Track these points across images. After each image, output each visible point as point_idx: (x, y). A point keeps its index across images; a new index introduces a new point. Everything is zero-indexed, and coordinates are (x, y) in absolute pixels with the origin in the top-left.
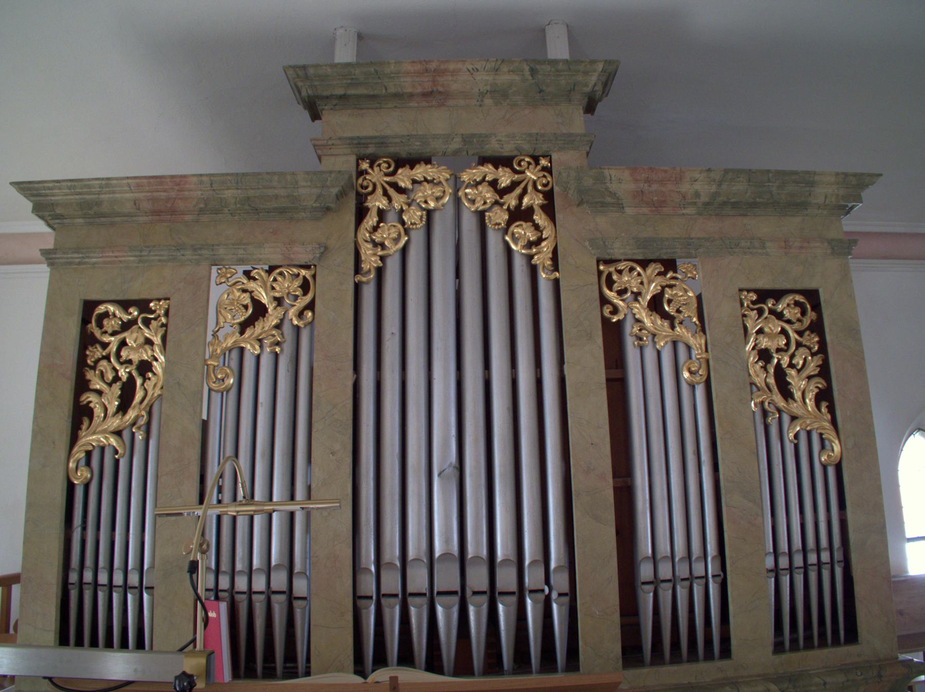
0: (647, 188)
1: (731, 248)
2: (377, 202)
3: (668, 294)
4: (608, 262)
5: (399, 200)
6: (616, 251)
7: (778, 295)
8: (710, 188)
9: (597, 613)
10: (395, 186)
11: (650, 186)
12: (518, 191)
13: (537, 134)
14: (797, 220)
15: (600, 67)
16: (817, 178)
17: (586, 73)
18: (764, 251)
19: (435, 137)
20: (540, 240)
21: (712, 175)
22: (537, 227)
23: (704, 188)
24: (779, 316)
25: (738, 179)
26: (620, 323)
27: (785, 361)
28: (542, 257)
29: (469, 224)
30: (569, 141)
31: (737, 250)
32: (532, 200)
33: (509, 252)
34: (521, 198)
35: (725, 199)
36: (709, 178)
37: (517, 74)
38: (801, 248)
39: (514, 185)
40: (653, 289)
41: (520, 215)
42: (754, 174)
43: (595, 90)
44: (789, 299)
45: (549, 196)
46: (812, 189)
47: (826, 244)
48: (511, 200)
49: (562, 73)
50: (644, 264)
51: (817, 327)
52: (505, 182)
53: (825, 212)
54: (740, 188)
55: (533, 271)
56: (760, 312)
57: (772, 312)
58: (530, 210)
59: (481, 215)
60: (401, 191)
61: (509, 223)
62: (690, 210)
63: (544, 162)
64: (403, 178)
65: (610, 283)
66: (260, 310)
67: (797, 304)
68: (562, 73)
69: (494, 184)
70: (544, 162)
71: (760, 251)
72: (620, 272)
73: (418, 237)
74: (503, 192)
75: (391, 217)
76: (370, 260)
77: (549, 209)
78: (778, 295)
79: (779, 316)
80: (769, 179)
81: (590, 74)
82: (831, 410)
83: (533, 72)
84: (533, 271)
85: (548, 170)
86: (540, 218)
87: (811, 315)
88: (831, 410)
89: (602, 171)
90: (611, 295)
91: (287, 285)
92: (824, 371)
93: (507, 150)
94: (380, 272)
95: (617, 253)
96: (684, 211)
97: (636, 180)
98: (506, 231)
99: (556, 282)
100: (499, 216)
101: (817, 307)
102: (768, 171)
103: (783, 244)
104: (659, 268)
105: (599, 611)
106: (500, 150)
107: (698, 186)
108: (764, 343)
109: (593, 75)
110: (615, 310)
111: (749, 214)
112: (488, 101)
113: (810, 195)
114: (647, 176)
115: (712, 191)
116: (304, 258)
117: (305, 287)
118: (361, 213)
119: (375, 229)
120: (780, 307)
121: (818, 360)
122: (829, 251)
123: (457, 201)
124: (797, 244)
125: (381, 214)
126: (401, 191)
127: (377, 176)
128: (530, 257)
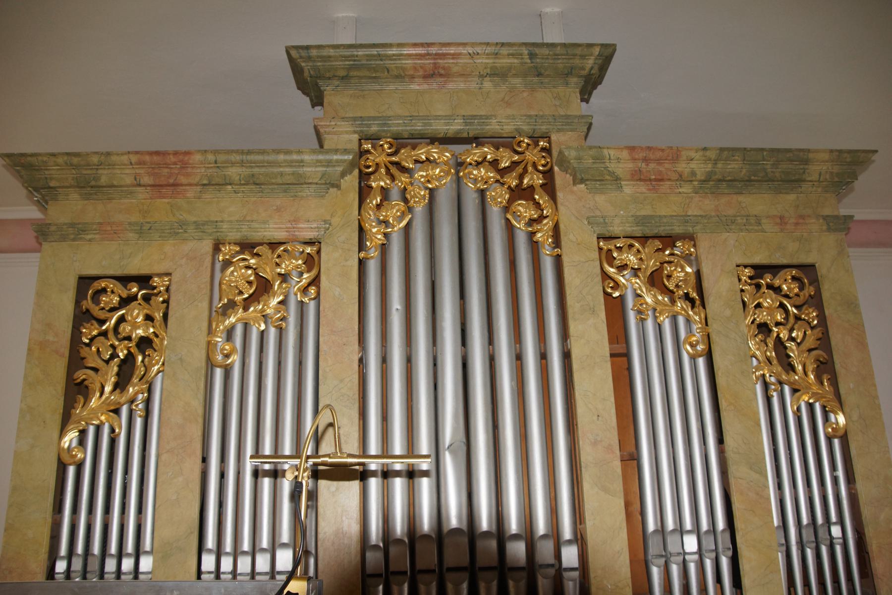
0: (645, 167)
1: (727, 225)
3: (668, 268)
6: (616, 228)
8: (705, 166)
9: (610, 587)
11: (647, 165)
12: (520, 169)
13: (536, 116)
14: (792, 197)
15: (597, 50)
16: (811, 156)
17: (583, 57)
18: (760, 228)
19: (437, 117)
20: (542, 217)
21: (708, 153)
22: (538, 205)
23: (700, 168)
24: (777, 290)
25: (733, 158)
27: (784, 335)
30: (567, 122)
31: (733, 227)
32: (534, 179)
33: (510, 229)
34: (521, 177)
35: (720, 177)
36: (706, 156)
37: (517, 58)
38: (797, 224)
39: (515, 164)
40: (652, 264)
41: (521, 193)
42: (748, 153)
43: (591, 73)
44: (789, 274)
45: (548, 174)
46: (806, 167)
47: (821, 221)
49: (560, 57)
50: (644, 239)
51: (816, 301)
52: (504, 164)
53: (819, 190)
54: (735, 166)
55: (534, 247)
56: (758, 286)
57: (770, 287)
58: (531, 188)
59: (482, 193)
60: (404, 170)
61: (510, 201)
62: (686, 189)
64: (406, 157)
65: (611, 260)
67: (794, 278)
68: (560, 57)
69: (494, 163)
71: (756, 228)
72: (619, 249)
74: (503, 172)
76: (376, 233)
77: (549, 188)
78: (774, 269)
79: (777, 290)
80: (763, 157)
81: (587, 57)
82: (834, 383)
83: (532, 56)
84: (534, 247)
87: (810, 290)
89: (602, 150)
92: (824, 342)
94: (384, 249)
95: (617, 230)
96: (681, 190)
97: (634, 159)
99: (558, 261)
100: (498, 196)
101: (815, 281)
102: (762, 150)
103: (778, 221)
105: (611, 585)
106: (501, 131)
107: (693, 165)
109: (590, 59)
110: (617, 286)
111: (744, 192)
113: (804, 172)
114: (645, 155)
115: (707, 170)
116: (309, 235)
119: (379, 206)
120: (777, 282)
121: (818, 332)
122: (825, 228)
123: (458, 180)
124: (793, 220)
125: (385, 192)
126: (404, 170)
128: (533, 234)
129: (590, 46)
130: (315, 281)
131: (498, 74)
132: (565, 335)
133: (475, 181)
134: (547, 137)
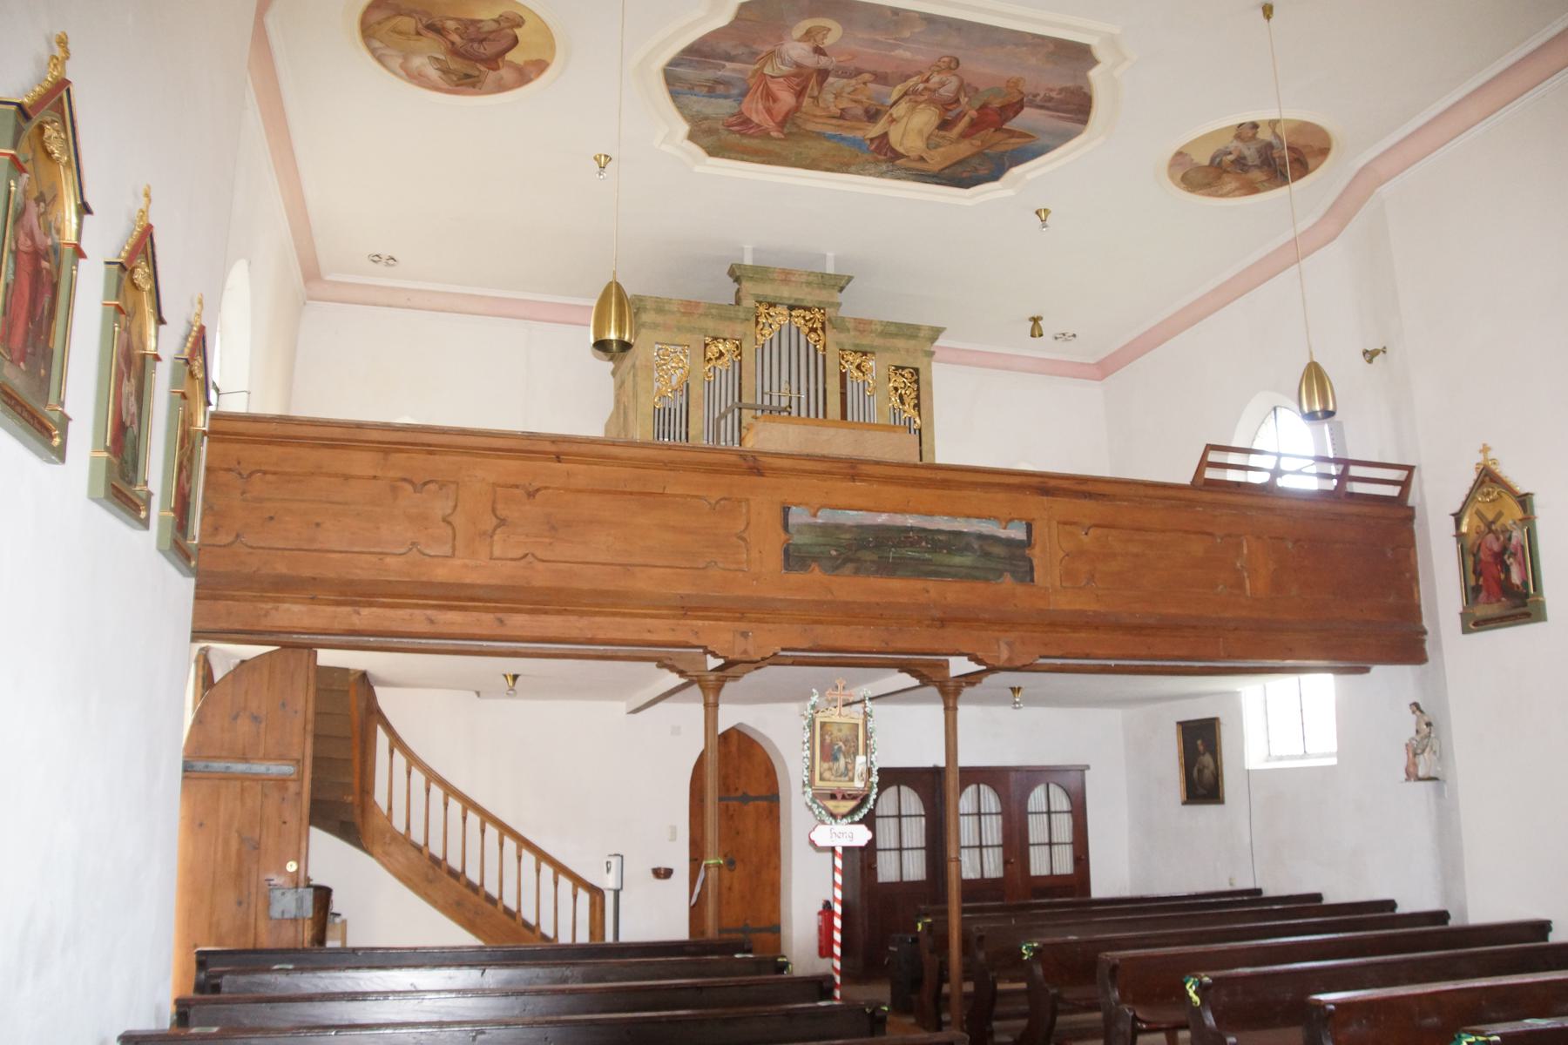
3: (863, 364)
4: (843, 350)
7: (903, 368)
10: (768, 314)
19: (785, 298)
20: (818, 341)
22: (819, 335)
23: (879, 328)
24: (903, 376)
26: (846, 372)
27: (903, 392)
29: (794, 331)
32: (817, 325)
39: (811, 319)
40: (858, 361)
41: (813, 330)
44: (907, 370)
45: (823, 323)
50: (856, 352)
51: (917, 382)
52: (807, 318)
55: (816, 351)
56: (896, 374)
57: (900, 374)
59: (798, 328)
60: (771, 316)
62: (873, 335)
63: (822, 311)
65: (843, 358)
66: (721, 354)
67: (910, 372)
70: (822, 311)
74: (807, 321)
75: (767, 325)
77: (823, 329)
78: (903, 368)
79: (903, 376)
82: (919, 411)
83: (822, 277)
84: (816, 351)
85: (824, 314)
86: (820, 332)
87: (915, 377)
88: (919, 411)
90: (843, 362)
92: (918, 397)
93: (810, 305)
95: (846, 347)
98: (807, 335)
99: (824, 356)
101: (918, 374)
104: (861, 354)
107: (877, 327)
108: (896, 385)
110: (844, 368)
112: (804, 285)
116: (738, 337)
117: (737, 347)
118: (757, 323)
119: (762, 329)
120: (903, 373)
121: (915, 393)
123: (790, 322)
128: (815, 346)
129: (844, 276)
130: (740, 354)
131: (809, 284)
132: (825, 383)
133: (796, 323)
134: (824, 309)
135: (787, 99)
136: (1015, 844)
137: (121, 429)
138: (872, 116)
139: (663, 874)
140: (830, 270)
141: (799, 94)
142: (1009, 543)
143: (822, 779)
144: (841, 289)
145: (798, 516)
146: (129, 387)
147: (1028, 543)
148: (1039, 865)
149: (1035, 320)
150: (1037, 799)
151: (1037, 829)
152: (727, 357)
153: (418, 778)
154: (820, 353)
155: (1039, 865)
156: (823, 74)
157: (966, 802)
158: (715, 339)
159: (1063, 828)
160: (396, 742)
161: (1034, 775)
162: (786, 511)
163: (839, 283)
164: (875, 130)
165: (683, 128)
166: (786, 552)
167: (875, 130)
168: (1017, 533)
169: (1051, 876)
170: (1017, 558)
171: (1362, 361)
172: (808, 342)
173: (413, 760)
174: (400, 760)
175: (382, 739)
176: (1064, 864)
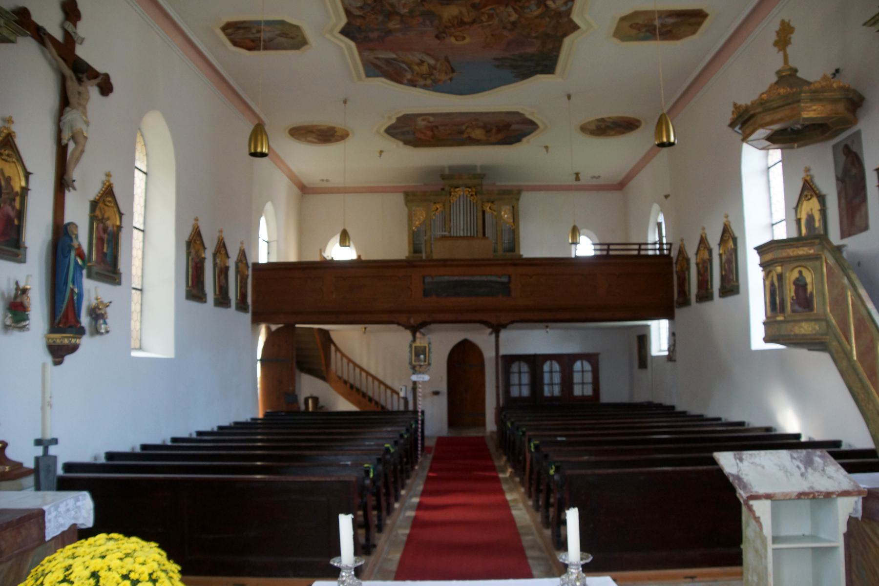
2: (453, 194)
5: (455, 193)
28: (475, 201)
29: (465, 197)
32: (474, 193)
41: (472, 195)
48: (471, 193)
73: (458, 199)
76: (452, 201)
84: (473, 203)
91: (441, 205)
94: (453, 204)
100: (469, 196)
118: (450, 195)
127: (452, 190)
135: (429, 133)
136: (567, 382)
137: (221, 287)
138: (462, 133)
139: (436, 393)
140: (479, 171)
141: (432, 131)
142: (502, 283)
143: (415, 361)
144: (482, 178)
145: (428, 280)
146: (222, 277)
147: (509, 282)
148: (577, 391)
149: (577, 174)
150: (578, 365)
151: (577, 378)
152: (439, 210)
153: (345, 360)
154: (475, 204)
155: (577, 391)
156: (437, 127)
157: (546, 367)
158: (435, 203)
159: (589, 377)
160: (337, 349)
161: (573, 358)
162: (424, 277)
163: (482, 176)
164: (465, 136)
165: (401, 144)
166: (424, 291)
167: (465, 136)
168: (505, 279)
169: (583, 396)
170: (505, 288)
171: (664, 198)
172: (470, 201)
173: (343, 355)
174: (339, 355)
175: (333, 348)
176: (588, 391)
